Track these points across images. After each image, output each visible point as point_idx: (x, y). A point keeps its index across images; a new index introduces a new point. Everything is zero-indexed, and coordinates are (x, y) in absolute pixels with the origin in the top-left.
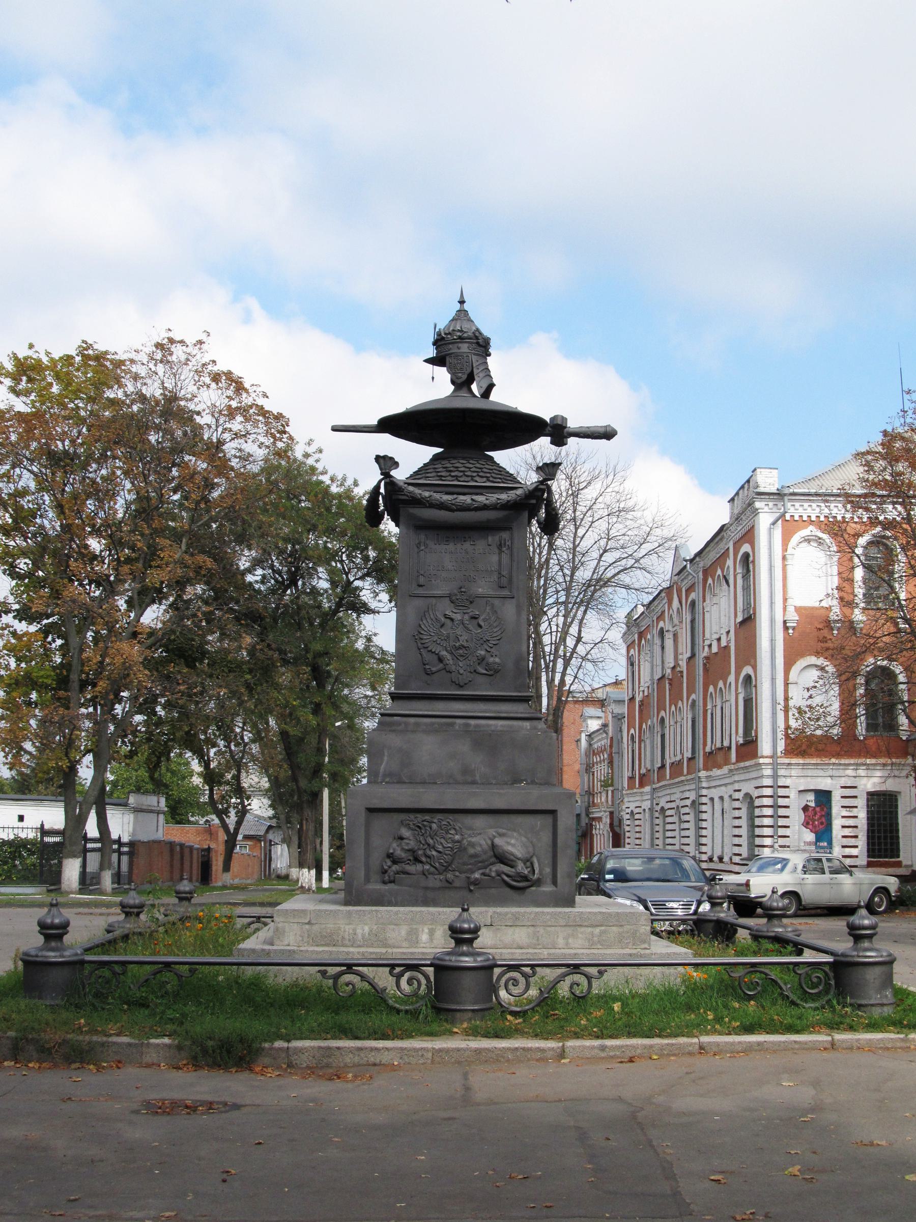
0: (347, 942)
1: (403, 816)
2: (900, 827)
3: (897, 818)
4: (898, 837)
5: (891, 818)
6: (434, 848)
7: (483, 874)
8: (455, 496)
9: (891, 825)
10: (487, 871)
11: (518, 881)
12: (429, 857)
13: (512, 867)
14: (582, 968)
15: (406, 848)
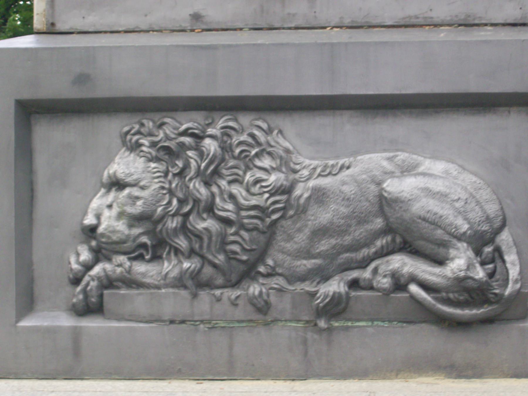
7: (354, 284)
13: (440, 262)
15: (129, 210)
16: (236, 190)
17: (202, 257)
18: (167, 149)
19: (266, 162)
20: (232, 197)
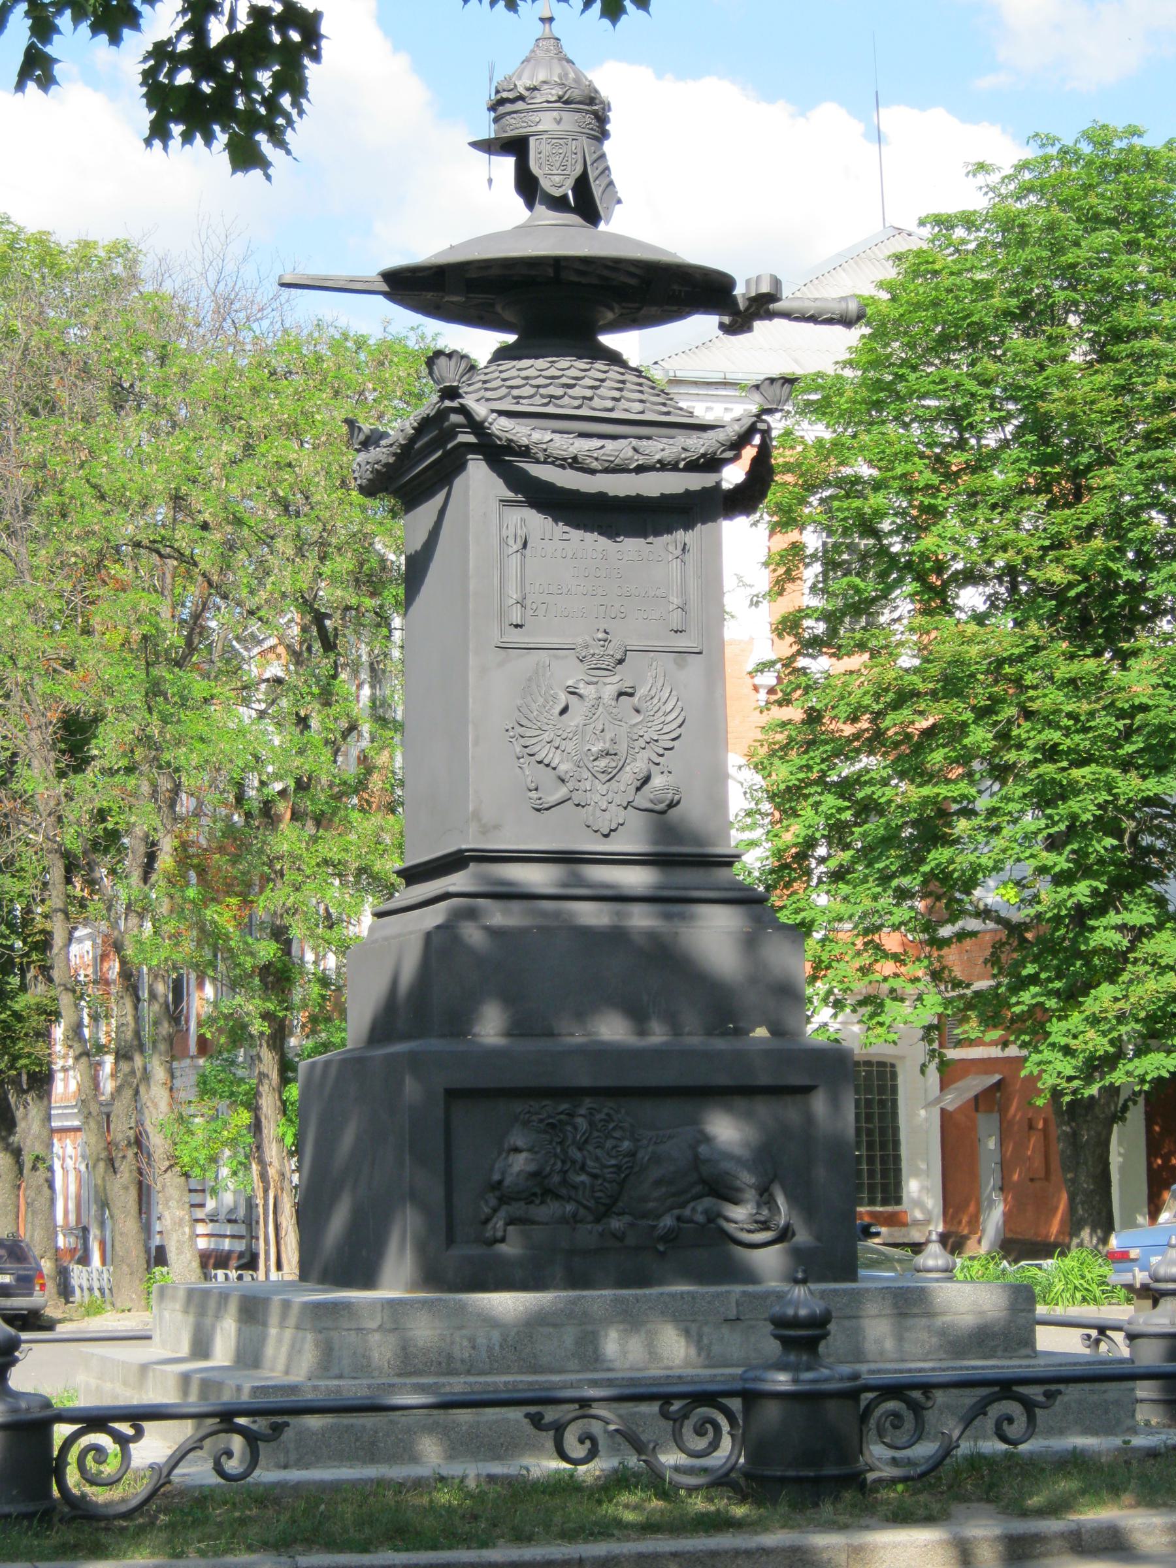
0: (458, 1365)
1: (518, 1107)
2: (903, 1136)
3: (895, 1115)
4: (897, 1159)
5: (882, 1117)
6: (583, 1168)
8: (597, 443)
9: (883, 1131)
10: (687, 1212)
11: (749, 1231)
12: (575, 1187)
14: (1015, 1388)
16: (599, 1152)
17: (577, 1202)
18: (553, 1126)
19: (617, 1134)
20: (597, 1159)
